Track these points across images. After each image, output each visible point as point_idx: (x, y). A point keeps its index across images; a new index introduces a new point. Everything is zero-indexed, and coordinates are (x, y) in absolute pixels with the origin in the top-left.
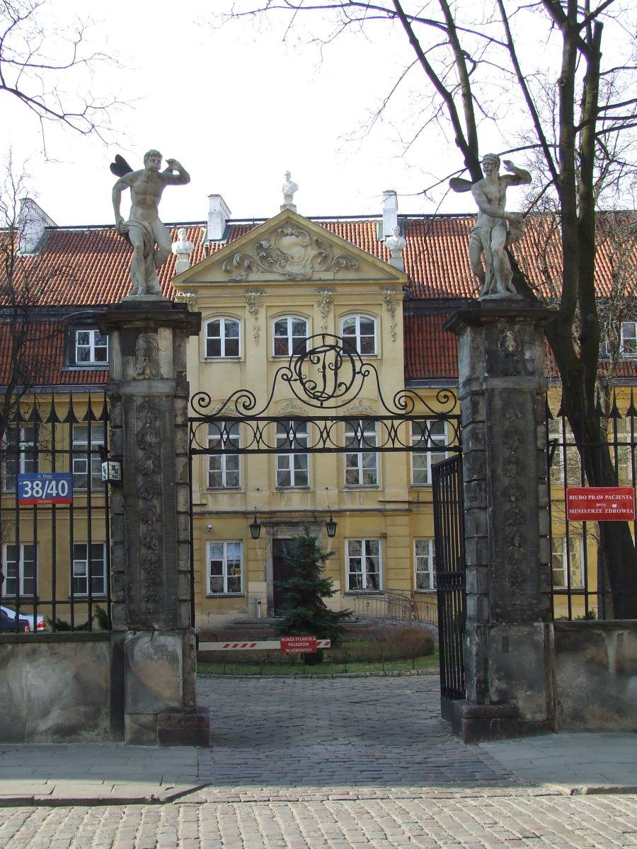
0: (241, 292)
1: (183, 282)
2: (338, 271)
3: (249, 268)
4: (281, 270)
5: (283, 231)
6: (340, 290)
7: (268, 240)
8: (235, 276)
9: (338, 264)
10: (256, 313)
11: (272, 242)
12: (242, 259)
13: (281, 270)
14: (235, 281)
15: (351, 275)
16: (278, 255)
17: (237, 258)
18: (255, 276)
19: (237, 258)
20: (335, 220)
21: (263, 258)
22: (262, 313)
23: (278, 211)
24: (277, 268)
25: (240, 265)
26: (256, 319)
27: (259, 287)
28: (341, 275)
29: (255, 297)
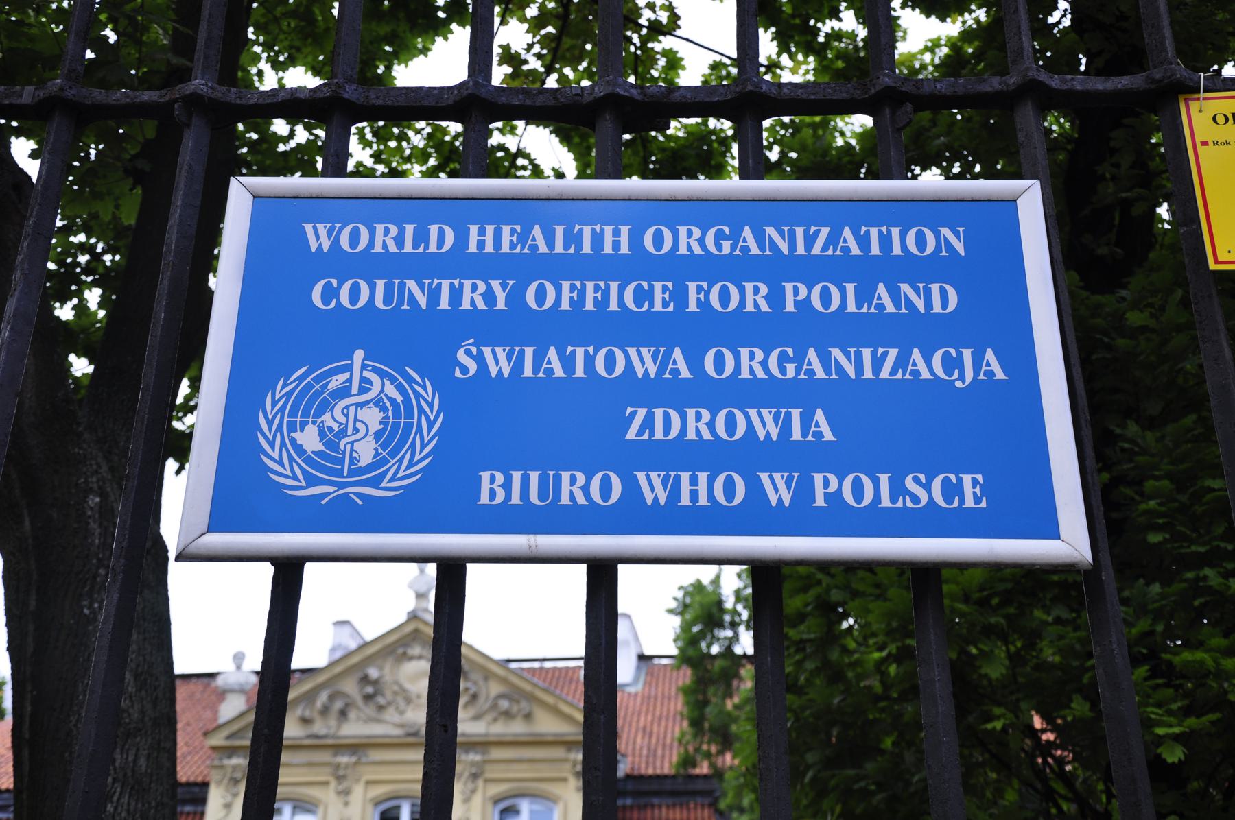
0: (325, 757)
1: (228, 737)
2: (495, 720)
3: (343, 714)
4: (396, 718)
5: (405, 654)
6: (496, 753)
7: (381, 668)
8: (319, 728)
9: (494, 706)
10: (346, 792)
11: (387, 670)
12: (332, 698)
13: (396, 718)
14: (317, 737)
15: (517, 728)
16: (395, 693)
17: (323, 698)
18: (353, 729)
19: (323, 698)
20: (536, 665)
21: (368, 698)
22: (358, 792)
23: (403, 618)
24: (391, 715)
25: (325, 711)
26: (346, 804)
27: (357, 747)
28: (499, 729)
29: (347, 766)
